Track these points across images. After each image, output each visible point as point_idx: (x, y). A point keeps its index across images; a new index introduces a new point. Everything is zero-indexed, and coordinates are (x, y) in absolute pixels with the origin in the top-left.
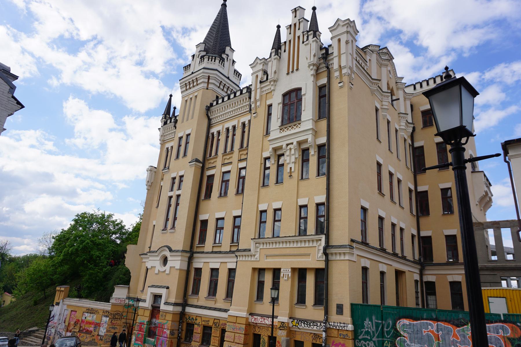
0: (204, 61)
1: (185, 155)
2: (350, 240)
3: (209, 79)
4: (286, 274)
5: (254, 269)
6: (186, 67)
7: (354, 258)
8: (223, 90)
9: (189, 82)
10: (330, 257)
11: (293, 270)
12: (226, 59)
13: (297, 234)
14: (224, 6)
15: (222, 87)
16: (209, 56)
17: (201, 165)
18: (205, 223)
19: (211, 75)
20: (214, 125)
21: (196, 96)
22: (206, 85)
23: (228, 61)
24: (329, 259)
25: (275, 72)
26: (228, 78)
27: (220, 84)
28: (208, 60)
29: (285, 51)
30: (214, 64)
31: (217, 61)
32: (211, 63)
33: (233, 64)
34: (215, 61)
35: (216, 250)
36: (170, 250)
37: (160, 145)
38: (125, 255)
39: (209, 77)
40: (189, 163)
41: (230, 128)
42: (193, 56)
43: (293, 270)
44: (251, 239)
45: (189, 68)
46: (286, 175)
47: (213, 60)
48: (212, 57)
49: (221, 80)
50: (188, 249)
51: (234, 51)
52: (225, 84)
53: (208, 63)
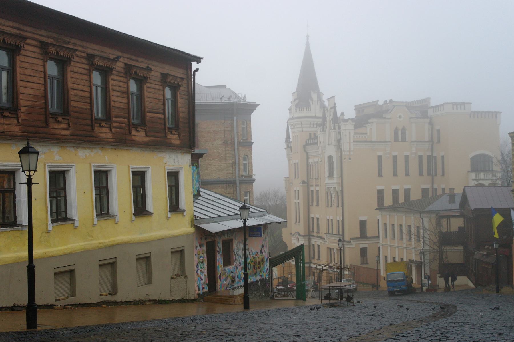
1: (298, 178)
2: (350, 239)
4: (335, 250)
5: (328, 248)
7: (354, 246)
8: (313, 127)
9: (292, 124)
10: (345, 246)
11: (337, 249)
12: (311, 103)
13: (338, 234)
14: (308, 44)
15: (312, 126)
17: (306, 184)
18: (313, 218)
19: (302, 122)
20: (309, 156)
21: (298, 136)
22: (301, 129)
23: (313, 104)
24: (345, 246)
25: (323, 142)
27: (310, 125)
29: (327, 128)
31: (305, 110)
33: (318, 104)
34: (303, 111)
35: (318, 235)
36: (300, 235)
37: (288, 161)
38: (282, 235)
39: (301, 123)
40: (300, 184)
41: (316, 162)
42: (292, 102)
43: (337, 249)
44: (325, 233)
46: (333, 203)
47: (302, 110)
50: (307, 234)
52: (314, 123)
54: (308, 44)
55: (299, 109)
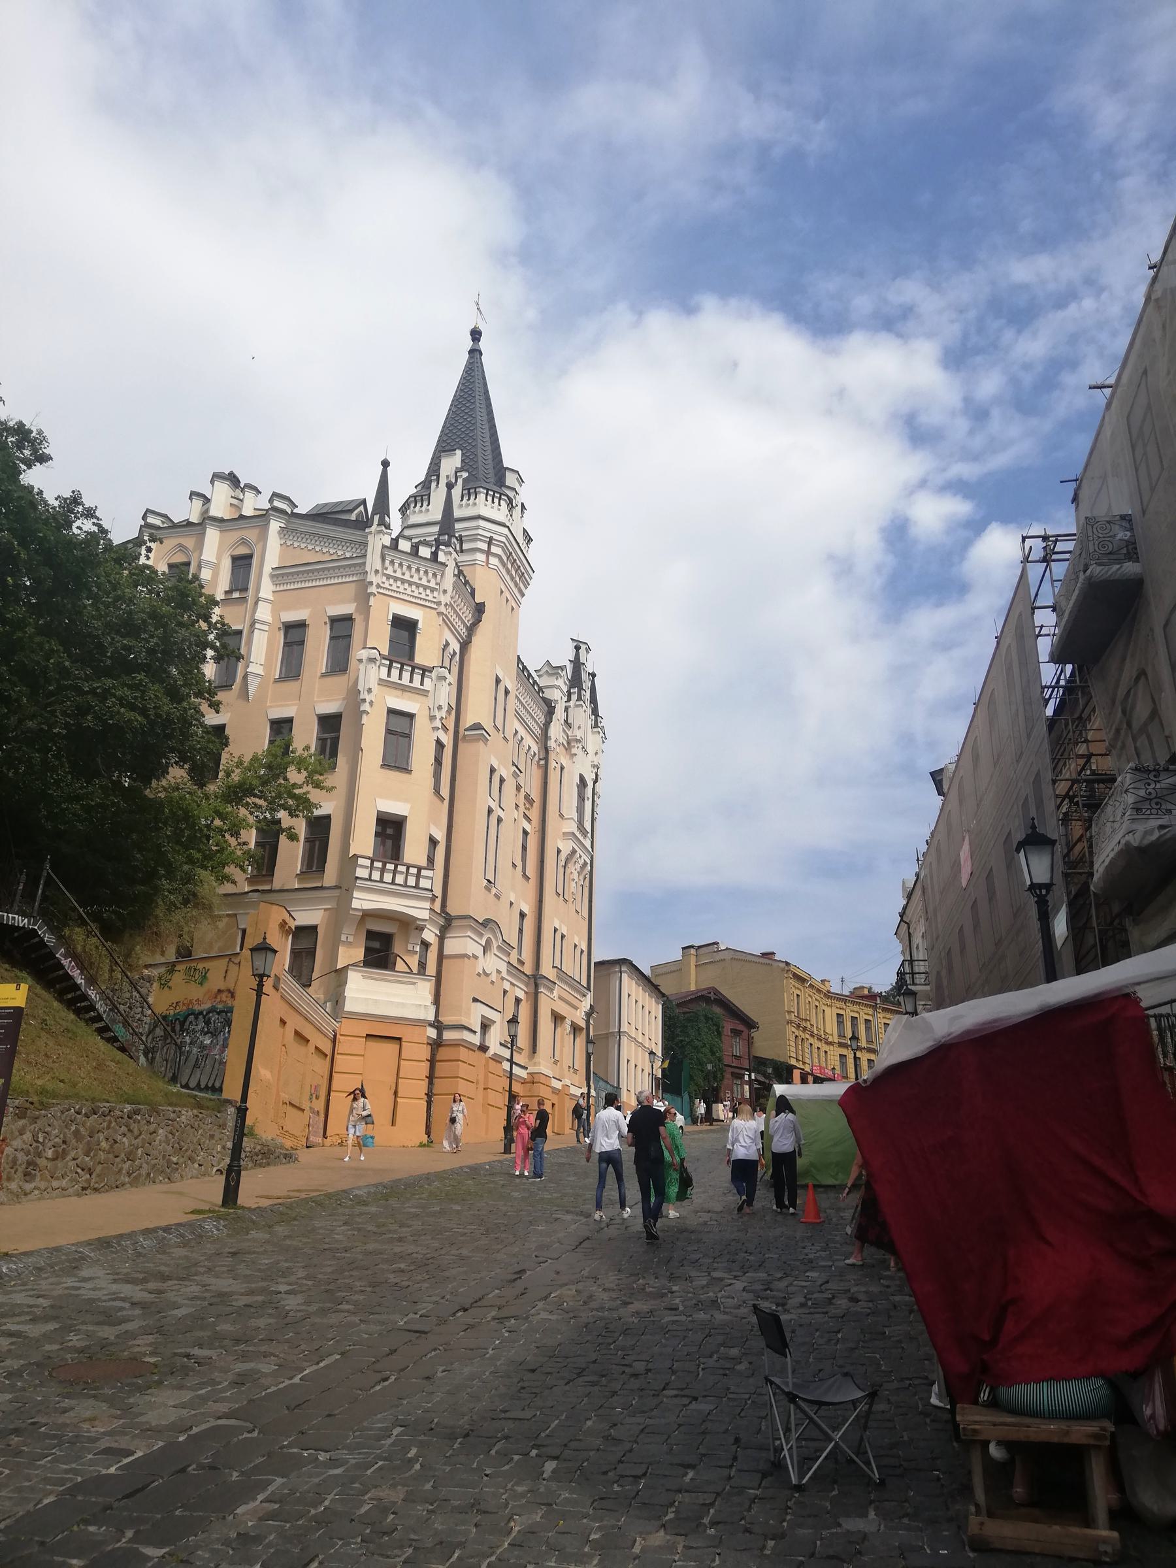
0: (476, 498)
3: (490, 544)
6: (414, 496)
16: (488, 490)
19: (495, 537)
26: (518, 544)
28: (487, 500)
30: (499, 510)
32: (493, 508)
34: (500, 505)
39: (491, 538)
45: (425, 503)
47: (496, 500)
48: (494, 492)
49: (511, 550)
51: (523, 481)
53: (486, 505)
54: (475, 353)
55: (487, 494)
